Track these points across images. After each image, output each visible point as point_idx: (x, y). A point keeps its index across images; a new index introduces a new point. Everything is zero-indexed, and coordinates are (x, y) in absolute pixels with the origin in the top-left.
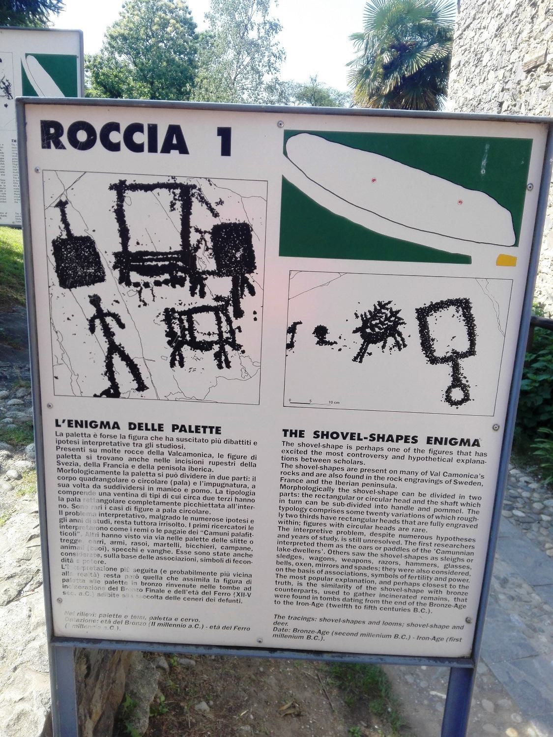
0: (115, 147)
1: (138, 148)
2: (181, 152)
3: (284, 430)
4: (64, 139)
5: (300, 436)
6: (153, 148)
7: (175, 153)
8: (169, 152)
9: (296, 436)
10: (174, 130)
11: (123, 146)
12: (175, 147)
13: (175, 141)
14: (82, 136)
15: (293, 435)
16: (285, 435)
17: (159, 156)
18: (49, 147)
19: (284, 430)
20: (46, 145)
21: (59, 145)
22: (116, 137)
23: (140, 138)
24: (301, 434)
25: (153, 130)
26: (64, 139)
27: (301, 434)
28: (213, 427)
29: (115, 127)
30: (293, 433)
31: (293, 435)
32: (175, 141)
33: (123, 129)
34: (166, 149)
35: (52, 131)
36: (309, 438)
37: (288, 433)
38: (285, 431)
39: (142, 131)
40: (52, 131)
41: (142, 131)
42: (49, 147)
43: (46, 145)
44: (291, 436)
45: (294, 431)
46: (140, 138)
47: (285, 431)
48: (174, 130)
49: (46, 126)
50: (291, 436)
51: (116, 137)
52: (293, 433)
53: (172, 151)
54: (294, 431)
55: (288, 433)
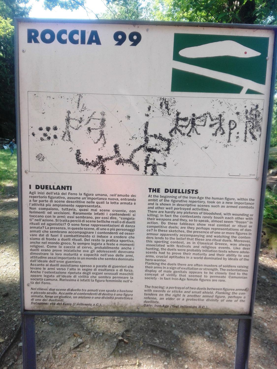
0: (64, 42)
1: (75, 42)
2: (97, 44)
3: (149, 189)
4: (39, 38)
5: (158, 192)
6: (83, 42)
7: (94, 44)
9: (156, 192)
10: (94, 34)
11: (68, 41)
12: (94, 42)
13: (94, 39)
14: (48, 36)
15: (154, 191)
16: (150, 191)
17: (86, 46)
19: (149, 189)
20: (29, 41)
21: (36, 41)
22: (64, 37)
24: (158, 190)
25: (83, 33)
26: (39, 38)
27: (158, 190)
29: (64, 32)
30: (154, 190)
31: (154, 191)
32: (94, 39)
34: (90, 42)
35: (33, 34)
36: (162, 192)
37: (152, 190)
38: (150, 189)
39: (78, 34)
40: (33, 34)
41: (78, 34)
43: (29, 41)
44: (153, 192)
45: (154, 189)
46: (77, 37)
47: (150, 189)
48: (94, 34)
49: (30, 31)
50: (153, 192)
52: (154, 190)
53: (93, 43)
54: (154, 189)
55: (152, 190)
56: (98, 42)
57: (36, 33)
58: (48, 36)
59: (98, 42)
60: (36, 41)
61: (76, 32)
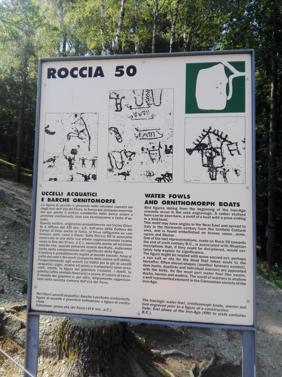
0: (75, 76)
1: (84, 76)
2: (101, 77)
4: (56, 75)
6: (90, 75)
7: (99, 77)
8: (96, 77)
10: (99, 69)
11: (79, 76)
12: (99, 75)
13: (99, 72)
17: (93, 78)
18: (50, 78)
20: (49, 77)
21: (54, 77)
22: (76, 73)
23: (85, 72)
25: (91, 69)
26: (56, 75)
28: (157, 194)
29: (76, 69)
32: (99, 72)
33: (79, 69)
34: (96, 75)
35: (52, 72)
40: (52, 72)
42: (50, 78)
43: (49, 77)
46: (85, 72)
48: (99, 69)
49: (49, 70)
51: (76, 73)
56: (102, 75)
57: (54, 70)
58: (63, 73)
59: (102, 75)
60: (54, 77)
61: (85, 68)
